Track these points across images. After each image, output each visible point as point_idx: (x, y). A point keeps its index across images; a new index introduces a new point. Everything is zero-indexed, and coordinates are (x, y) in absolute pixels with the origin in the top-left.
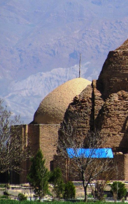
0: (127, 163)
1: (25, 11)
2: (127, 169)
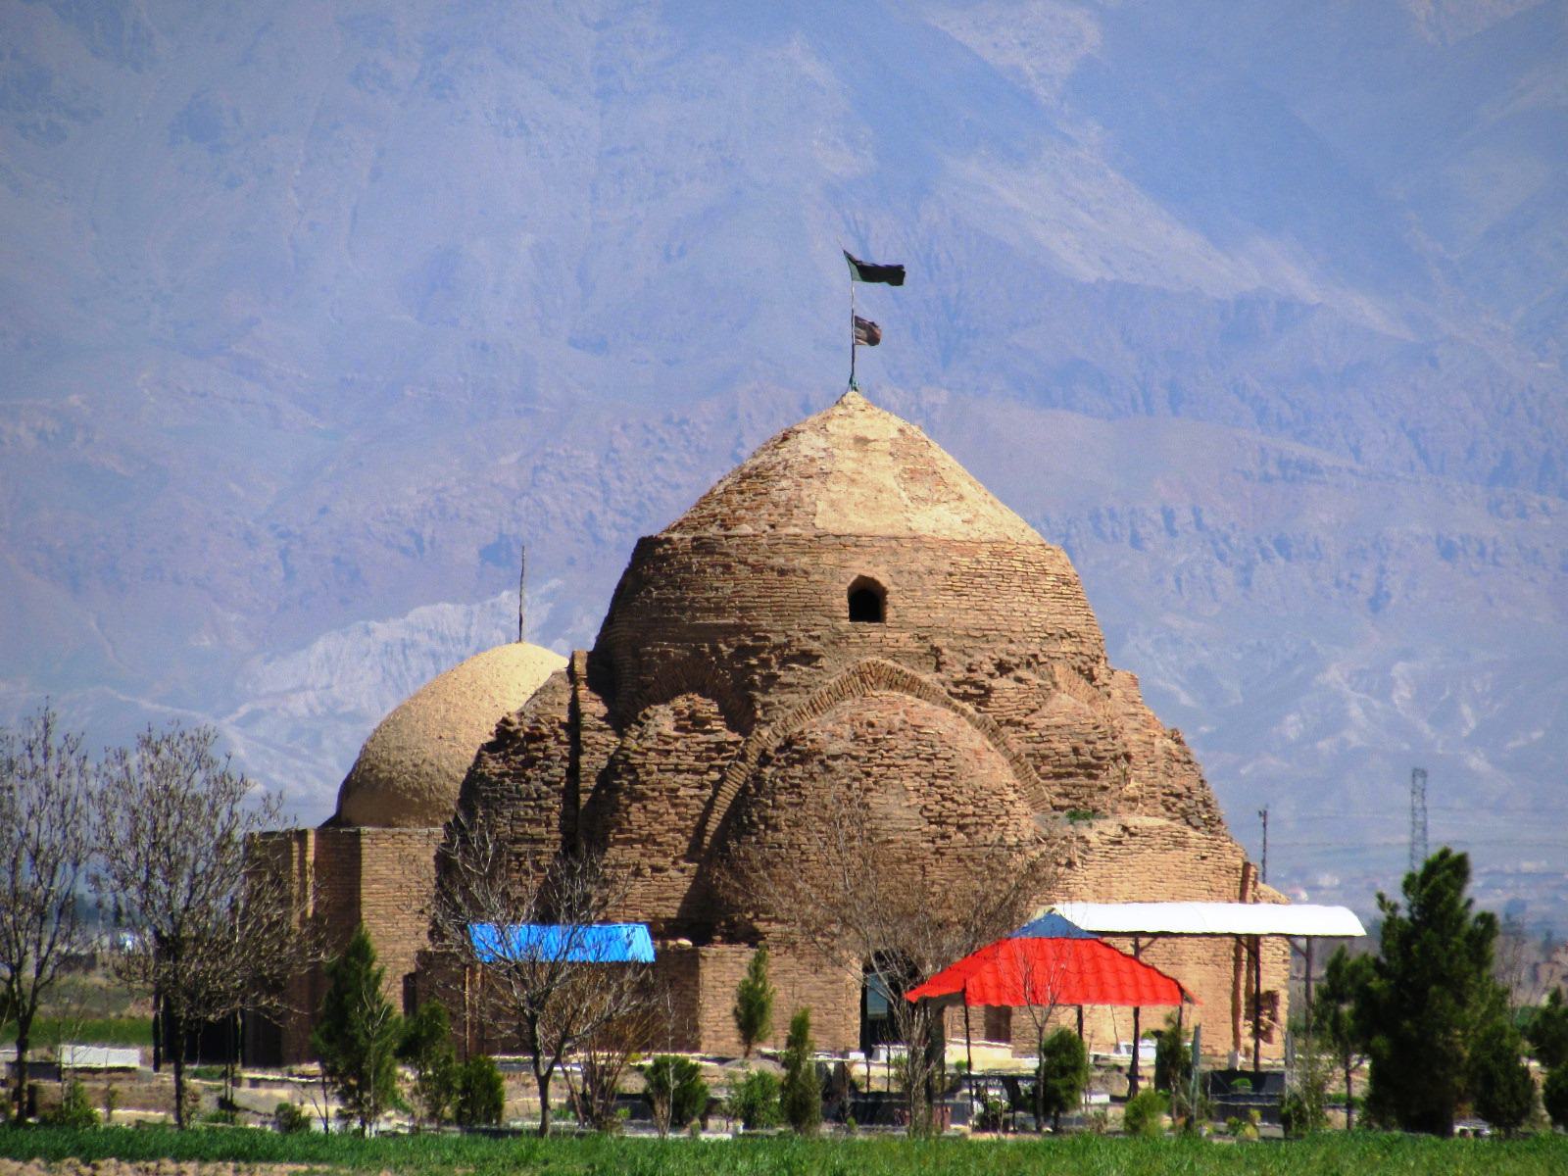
0: (1048, 1167)
1: (305, 376)
2: (929, 1169)
